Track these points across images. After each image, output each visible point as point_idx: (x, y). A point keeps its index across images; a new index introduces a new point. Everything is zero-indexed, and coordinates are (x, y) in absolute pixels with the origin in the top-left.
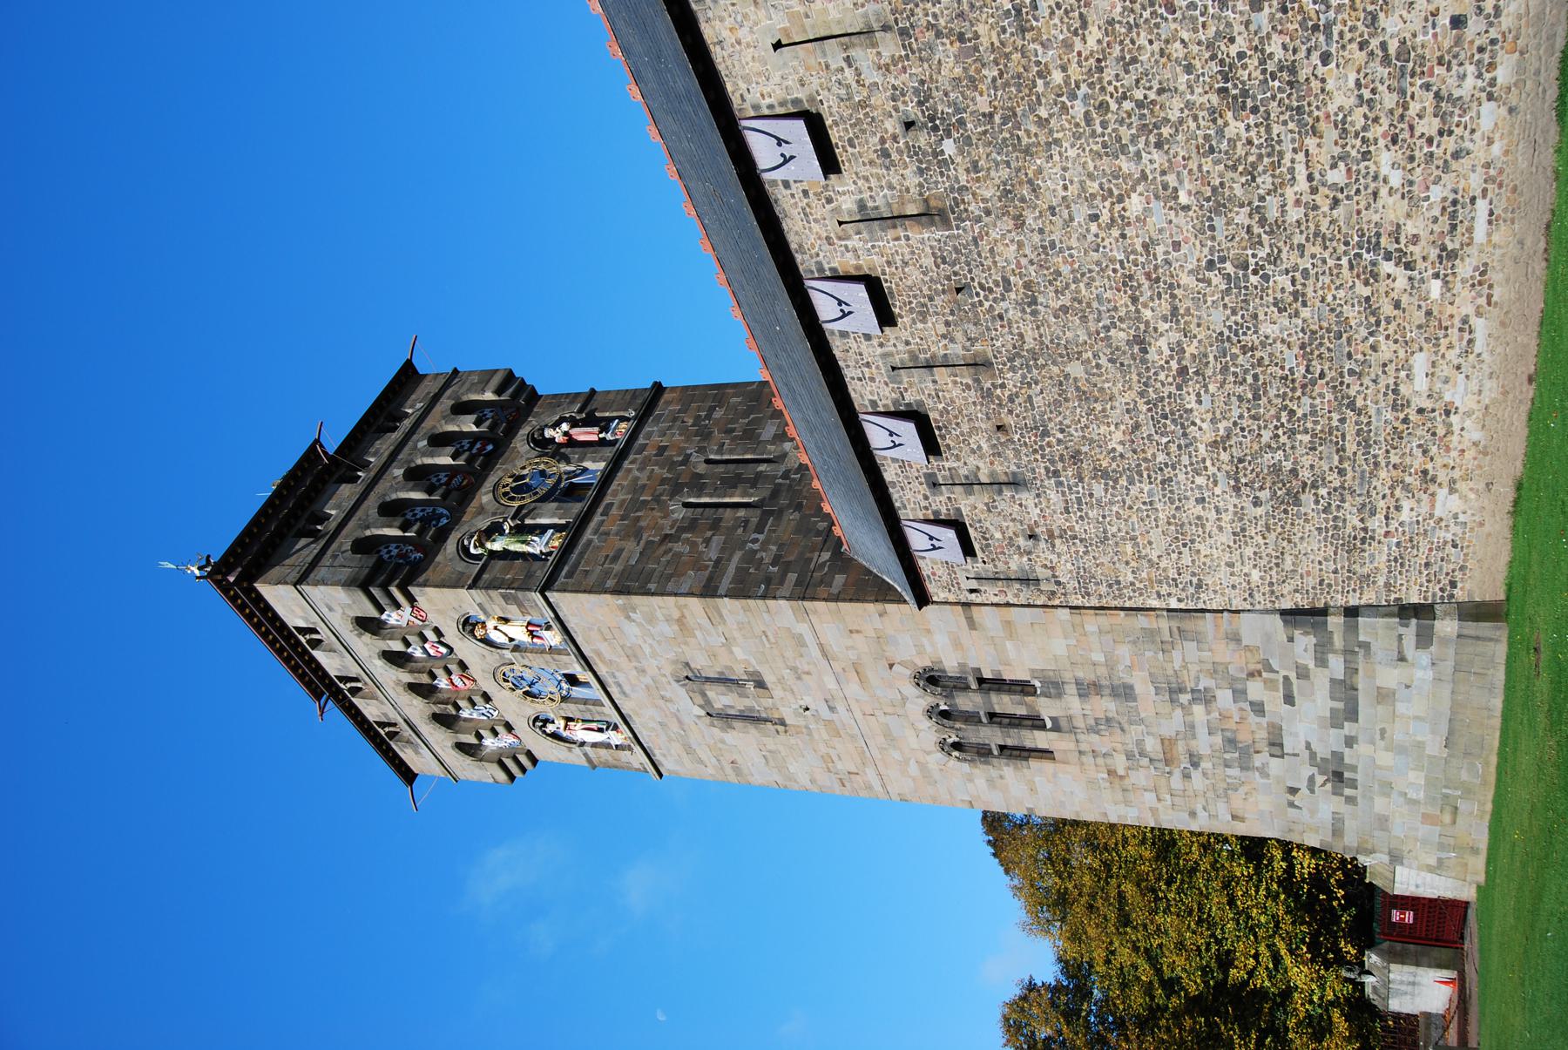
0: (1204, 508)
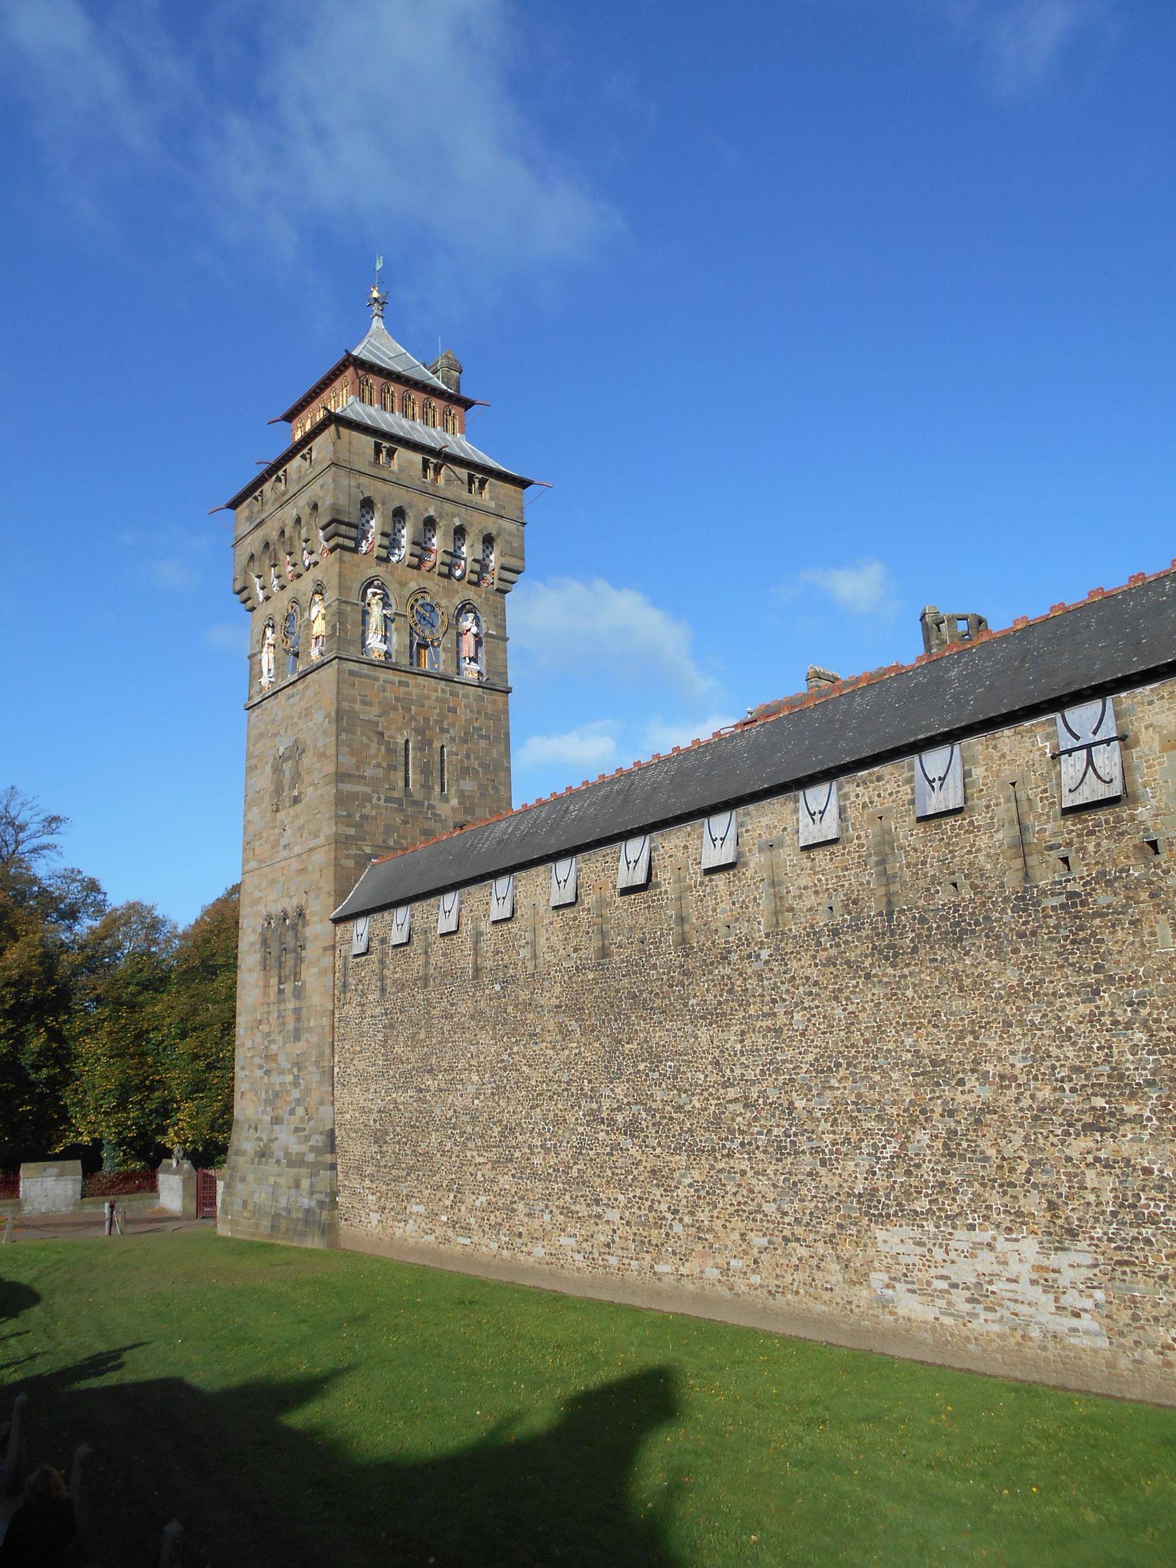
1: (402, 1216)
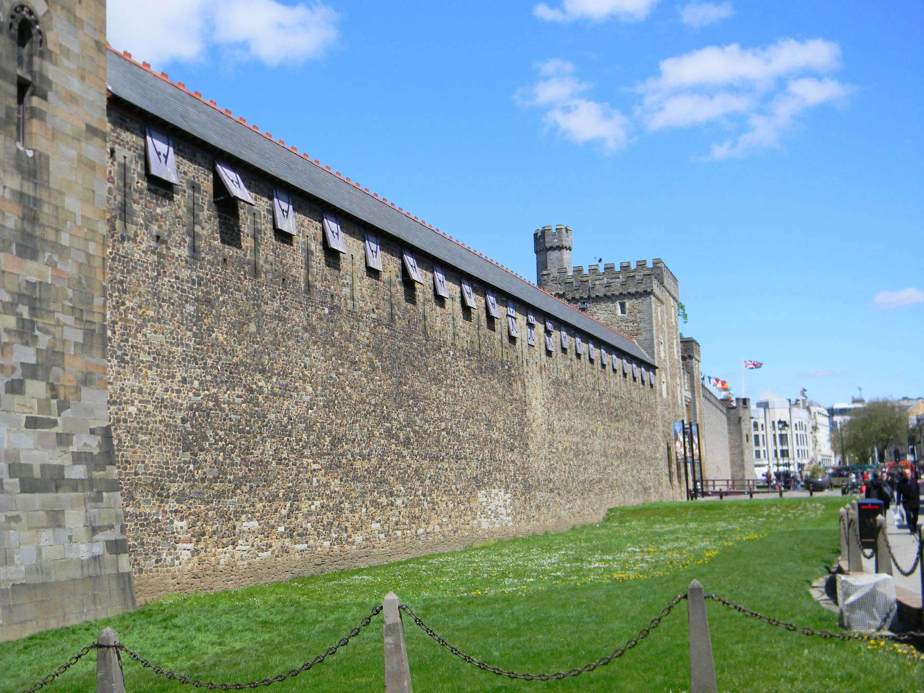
0: (179, 381)
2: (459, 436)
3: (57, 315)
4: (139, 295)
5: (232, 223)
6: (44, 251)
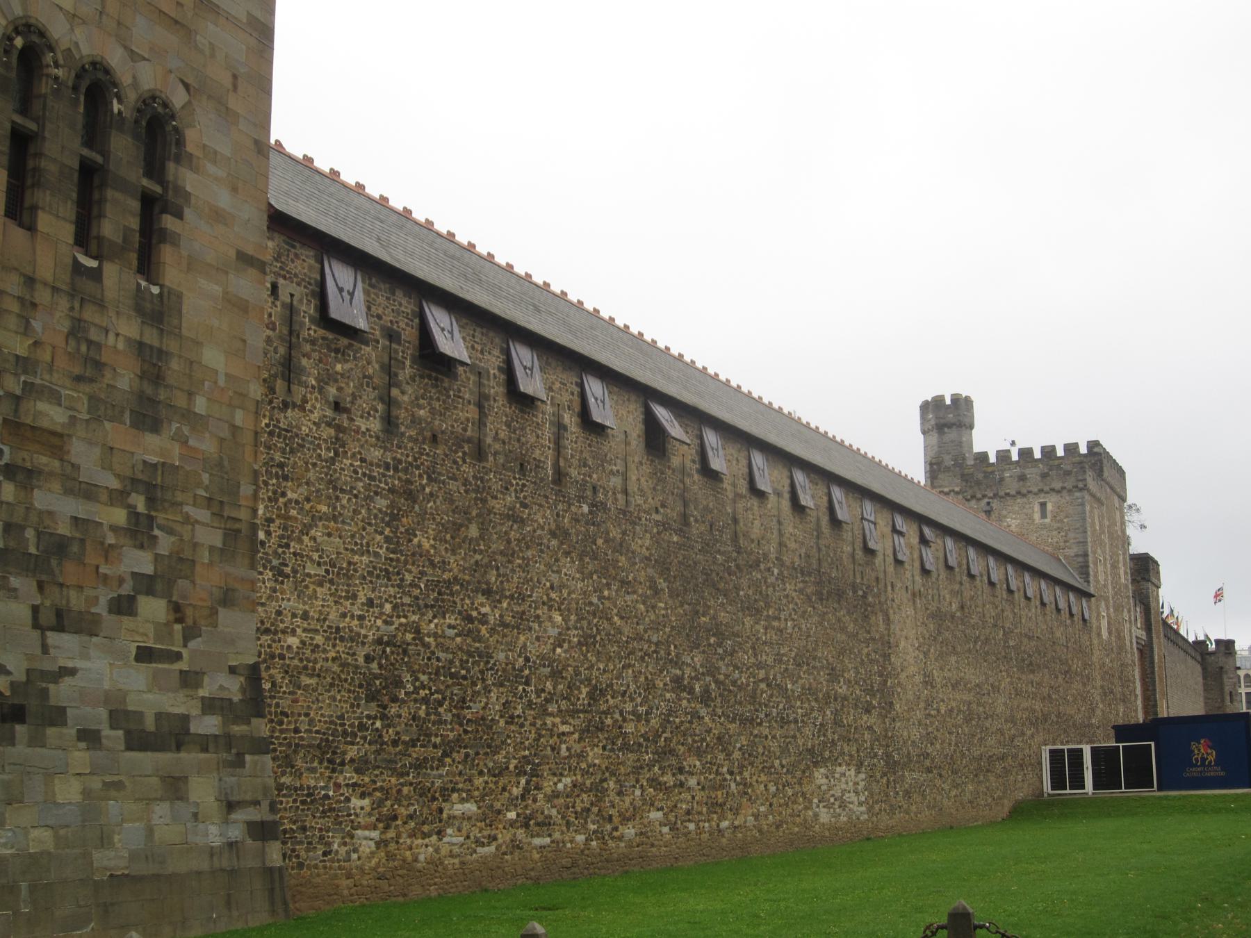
0: (363, 604)
1: (437, 824)
2: (787, 689)
3: (186, 509)
4: (307, 484)
5: (446, 385)
6: (170, 422)
